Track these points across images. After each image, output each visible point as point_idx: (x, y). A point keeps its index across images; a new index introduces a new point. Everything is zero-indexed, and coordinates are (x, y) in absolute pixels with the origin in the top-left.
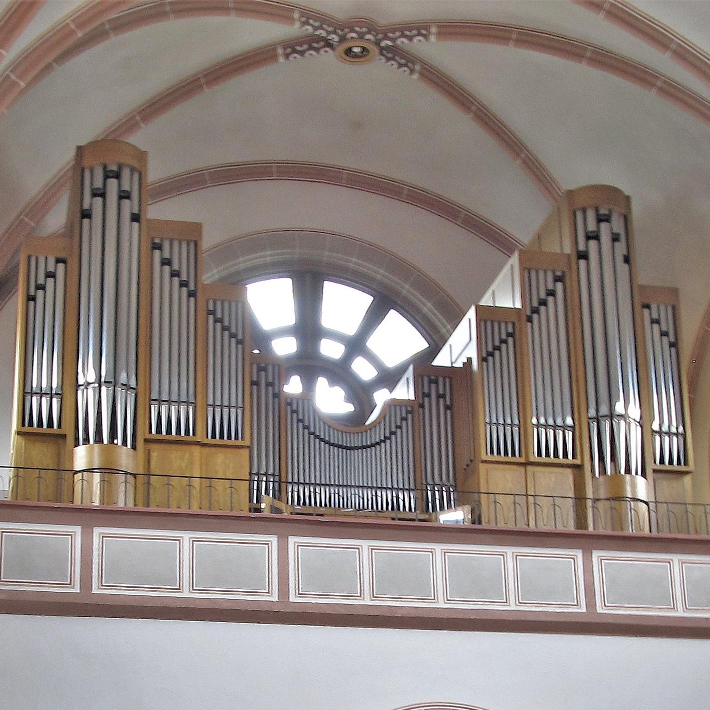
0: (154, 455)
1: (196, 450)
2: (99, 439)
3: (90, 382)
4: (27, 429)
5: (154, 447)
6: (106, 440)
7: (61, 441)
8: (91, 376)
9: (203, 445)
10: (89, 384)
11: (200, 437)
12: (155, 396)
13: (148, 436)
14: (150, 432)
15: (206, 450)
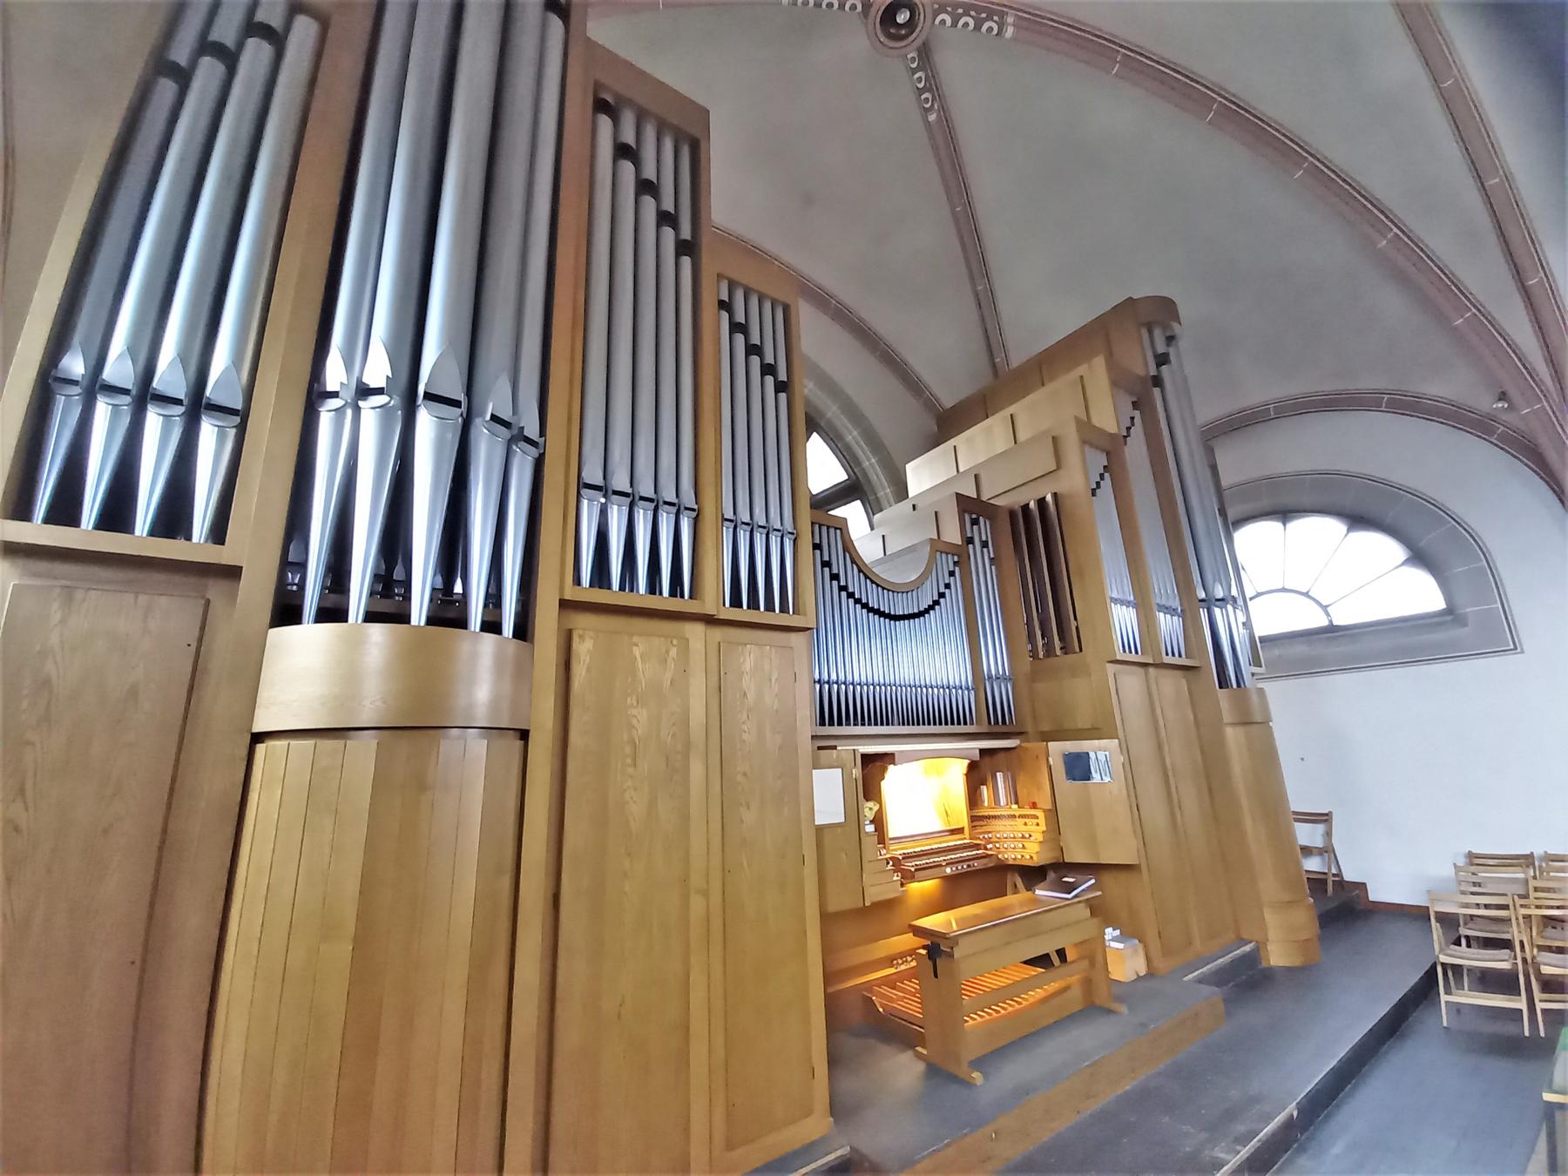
0: (583, 649)
1: (695, 631)
2: (389, 604)
3: (373, 385)
4: (35, 532)
5: (582, 621)
6: (419, 609)
7: (215, 590)
8: (378, 370)
9: (710, 620)
10: (364, 391)
11: (709, 605)
12: (593, 475)
13: (571, 593)
14: (577, 581)
15: (717, 634)
